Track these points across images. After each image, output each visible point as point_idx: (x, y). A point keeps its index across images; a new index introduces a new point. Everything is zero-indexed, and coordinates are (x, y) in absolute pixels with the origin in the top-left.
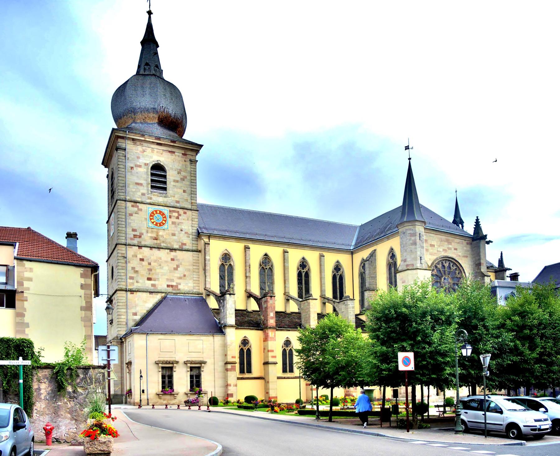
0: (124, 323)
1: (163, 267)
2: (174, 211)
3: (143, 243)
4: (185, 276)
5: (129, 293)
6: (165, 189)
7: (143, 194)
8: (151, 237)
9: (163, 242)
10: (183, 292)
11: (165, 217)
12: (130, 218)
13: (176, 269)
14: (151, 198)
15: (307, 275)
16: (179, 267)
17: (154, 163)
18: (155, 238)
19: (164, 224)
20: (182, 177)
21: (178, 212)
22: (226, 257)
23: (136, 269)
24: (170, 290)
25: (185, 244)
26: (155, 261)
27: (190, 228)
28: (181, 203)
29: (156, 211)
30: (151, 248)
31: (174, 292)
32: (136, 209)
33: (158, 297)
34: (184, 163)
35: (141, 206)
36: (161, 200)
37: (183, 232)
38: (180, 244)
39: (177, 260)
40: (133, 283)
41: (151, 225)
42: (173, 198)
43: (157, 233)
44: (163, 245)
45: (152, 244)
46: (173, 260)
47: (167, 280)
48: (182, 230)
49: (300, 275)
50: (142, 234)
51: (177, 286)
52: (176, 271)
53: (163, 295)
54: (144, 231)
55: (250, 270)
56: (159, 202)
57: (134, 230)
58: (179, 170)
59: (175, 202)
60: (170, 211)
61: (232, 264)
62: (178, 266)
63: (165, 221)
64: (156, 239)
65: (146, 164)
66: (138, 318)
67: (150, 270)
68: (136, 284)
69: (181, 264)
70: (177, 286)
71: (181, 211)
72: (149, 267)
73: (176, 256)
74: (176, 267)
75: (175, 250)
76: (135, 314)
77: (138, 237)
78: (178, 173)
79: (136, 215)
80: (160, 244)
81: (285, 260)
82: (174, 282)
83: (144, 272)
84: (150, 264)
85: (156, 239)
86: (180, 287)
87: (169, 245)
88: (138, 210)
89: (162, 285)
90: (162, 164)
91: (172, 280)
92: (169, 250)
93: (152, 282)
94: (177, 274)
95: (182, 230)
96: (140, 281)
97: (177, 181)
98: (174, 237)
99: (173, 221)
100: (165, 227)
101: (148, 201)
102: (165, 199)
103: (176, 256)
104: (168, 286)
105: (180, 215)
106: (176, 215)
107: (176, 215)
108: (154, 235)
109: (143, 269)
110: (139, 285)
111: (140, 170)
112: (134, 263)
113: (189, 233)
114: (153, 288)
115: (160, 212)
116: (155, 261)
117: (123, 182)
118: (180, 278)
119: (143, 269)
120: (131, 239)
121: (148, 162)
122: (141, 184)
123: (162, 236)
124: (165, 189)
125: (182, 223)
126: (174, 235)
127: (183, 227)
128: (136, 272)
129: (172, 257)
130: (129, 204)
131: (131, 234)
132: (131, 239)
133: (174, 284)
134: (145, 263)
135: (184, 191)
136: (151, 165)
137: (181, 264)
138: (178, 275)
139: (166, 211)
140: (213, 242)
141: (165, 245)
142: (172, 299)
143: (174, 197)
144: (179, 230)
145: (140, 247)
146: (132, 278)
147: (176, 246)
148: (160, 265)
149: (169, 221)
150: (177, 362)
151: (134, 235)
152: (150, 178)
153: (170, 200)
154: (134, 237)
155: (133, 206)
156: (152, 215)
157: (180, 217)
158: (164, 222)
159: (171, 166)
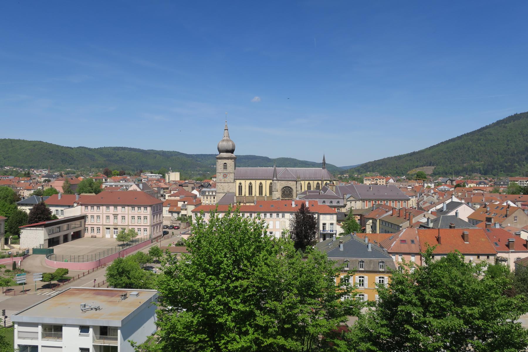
15: (262, 186)
22: (240, 184)
36: (225, 171)
49: (260, 186)
81: (255, 183)
89: (226, 191)
94: (229, 188)
112: (220, 187)
140: (237, 181)
147: (229, 182)
152: (223, 166)
153: (228, 171)
156: (224, 175)
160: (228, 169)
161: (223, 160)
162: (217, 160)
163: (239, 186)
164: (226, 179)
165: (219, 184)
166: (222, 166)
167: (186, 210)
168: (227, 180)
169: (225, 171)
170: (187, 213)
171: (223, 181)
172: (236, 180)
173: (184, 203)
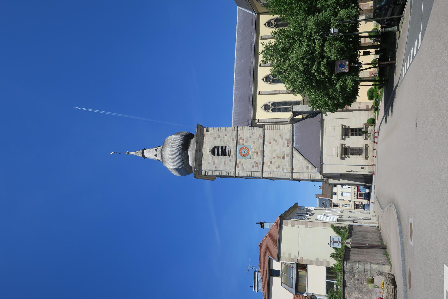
0: (314, 175)
1: (275, 149)
2: (239, 141)
3: (261, 161)
4: (280, 135)
5: (294, 171)
6: (226, 147)
7: (230, 161)
8: (256, 156)
9: (259, 149)
10: (291, 136)
11: (243, 147)
12: (245, 169)
13: (276, 141)
14: (233, 156)
16: (275, 139)
17: (211, 154)
18: (257, 154)
19: (248, 148)
20: (218, 137)
21: (240, 139)
22: (266, 107)
23: (278, 166)
24: (290, 145)
25: (260, 135)
26: (272, 154)
27: (249, 131)
28: (233, 138)
29: (240, 153)
30: (263, 156)
31: (291, 142)
32: (240, 165)
33: (295, 152)
34: (209, 135)
35: (238, 162)
36: (233, 151)
37: (252, 136)
38: (260, 138)
39: (270, 140)
40: (287, 168)
41: (249, 156)
42: (231, 142)
43: (253, 152)
44: (261, 149)
45: (261, 156)
46: (270, 143)
47: (283, 146)
48: (251, 137)
50: (255, 162)
51: (288, 140)
52: (278, 140)
53: (294, 149)
54: (253, 161)
55: (274, 91)
56: (234, 151)
57: (253, 167)
58: (214, 139)
59: (233, 141)
60: (239, 144)
61: (271, 103)
62: (274, 140)
63: (246, 147)
64: (257, 153)
65: (212, 159)
66: (310, 166)
67: (278, 157)
68: (287, 167)
69: (273, 137)
70: (288, 140)
71: (239, 137)
72: (276, 158)
73: (268, 140)
74: (275, 141)
75: (264, 141)
76: (307, 168)
77: (257, 164)
78: (216, 139)
79: (243, 165)
80: (261, 151)
82: (285, 142)
83: (279, 162)
84: (274, 158)
85: (257, 153)
86: (288, 138)
87: (261, 145)
88: (240, 164)
89: (288, 150)
90: (211, 149)
91: (284, 143)
92: (265, 145)
93: (286, 156)
94: (280, 140)
95: (251, 137)
96: (285, 164)
97: (221, 139)
98: (255, 142)
99: (245, 142)
100: (249, 148)
101: (234, 157)
102: (232, 147)
103: (268, 140)
104: (288, 146)
105: (241, 138)
106: (241, 140)
107: (241, 140)
108: (255, 154)
109: (277, 162)
110: (287, 165)
111: (216, 162)
112: (274, 168)
113: (252, 132)
114: (289, 156)
115: (240, 150)
116: (272, 154)
117: (224, 173)
118: (282, 138)
119: (277, 162)
120: (258, 169)
121: (211, 157)
122: (224, 162)
123: (255, 149)
124: (226, 147)
125: (246, 136)
126: (254, 142)
127: (249, 136)
128: (279, 166)
129: (269, 143)
130: (237, 169)
131: (255, 169)
132: (258, 169)
133: (286, 142)
134: (273, 161)
135: (226, 135)
136: (212, 156)
137: (273, 137)
138: (280, 139)
139: (239, 147)
140: (258, 117)
141: (261, 148)
142: (297, 144)
143: (230, 142)
144: (250, 138)
145: (263, 163)
146: (283, 169)
147: (261, 141)
148: (274, 151)
149: (245, 144)
150: (342, 145)
151: (256, 167)
152: (220, 156)
153: (233, 144)
154: (257, 167)
155: (238, 167)
157: (242, 138)
158: (246, 148)
159: (212, 144)
160: (227, 144)
161: (204, 157)
162: (203, 173)
163: (274, 110)
164: (253, 150)
165: (266, 169)
166: (219, 160)
167: (302, 267)
168: (255, 147)
169: (233, 151)
170: (318, 262)
171: (259, 159)
172: (254, 119)
173: (277, 273)
